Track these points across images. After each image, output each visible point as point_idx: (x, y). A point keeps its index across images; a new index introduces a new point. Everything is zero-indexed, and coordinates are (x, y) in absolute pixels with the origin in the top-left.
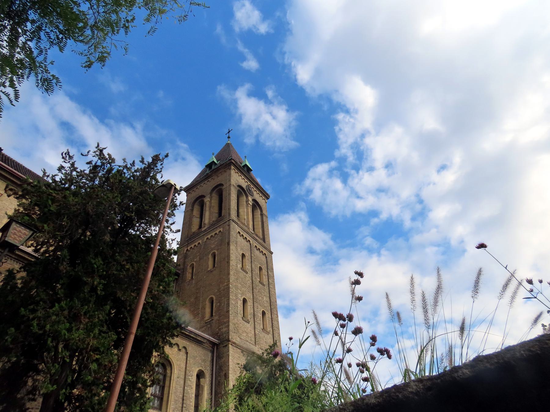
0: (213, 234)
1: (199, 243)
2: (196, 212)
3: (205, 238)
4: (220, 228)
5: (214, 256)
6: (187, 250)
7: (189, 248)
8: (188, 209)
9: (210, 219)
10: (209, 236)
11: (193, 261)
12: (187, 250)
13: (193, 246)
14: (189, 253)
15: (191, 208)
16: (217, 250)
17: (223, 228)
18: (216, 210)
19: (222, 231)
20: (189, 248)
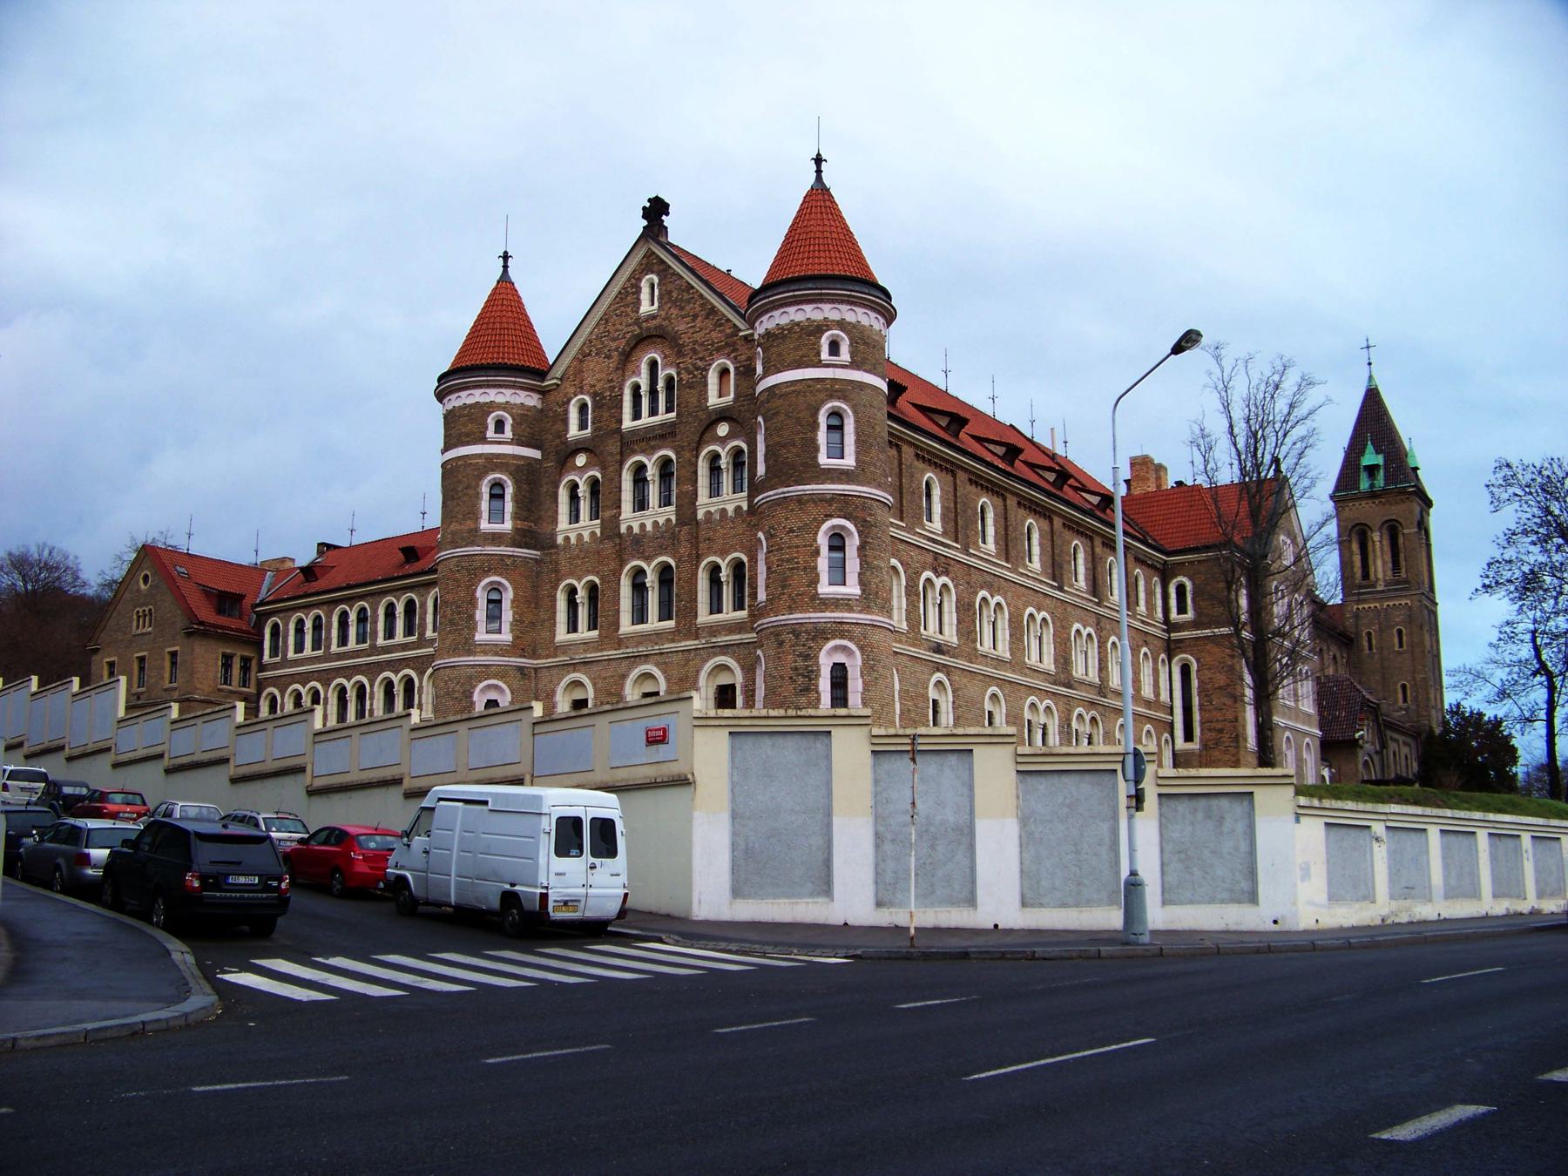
5: (1400, 632)
9: (1384, 572)
12: (1358, 609)
13: (1366, 606)
14: (1361, 614)
18: (1388, 558)
20: (1360, 607)
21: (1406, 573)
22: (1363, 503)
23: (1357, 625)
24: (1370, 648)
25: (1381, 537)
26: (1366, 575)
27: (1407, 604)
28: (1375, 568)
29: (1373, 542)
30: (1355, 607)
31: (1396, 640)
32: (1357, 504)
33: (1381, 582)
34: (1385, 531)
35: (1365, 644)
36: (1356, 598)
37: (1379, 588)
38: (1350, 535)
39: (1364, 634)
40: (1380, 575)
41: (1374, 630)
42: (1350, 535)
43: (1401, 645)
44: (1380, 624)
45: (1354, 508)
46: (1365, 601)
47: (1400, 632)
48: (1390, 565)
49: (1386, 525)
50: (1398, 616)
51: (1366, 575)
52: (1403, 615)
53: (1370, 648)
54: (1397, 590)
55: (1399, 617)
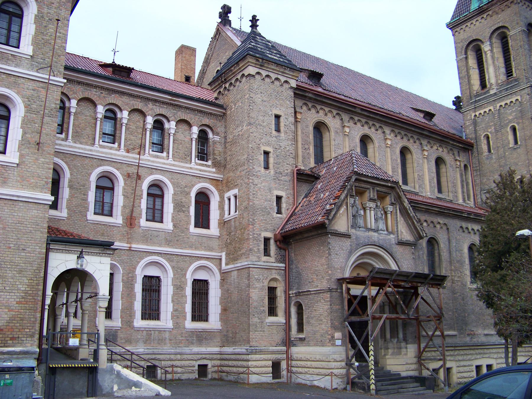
0: (508, 102)
1: (490, 110)
2: (472, 62)
3: (498, 105)
4: (517, 96)
5: (514, 129)
6: (475, 116)
7: (477, 114)
8: (461, 57)
9: (496, 77)
10: (503, 104)
11: (486, 130)
12: (475, 116)
13: (482, 112)
14: (479, 120)
15: (465, 56)
16: (518, 123)
17: (521, 96)
19: (520, 100)
20: (477, 114)
21: (515, 72)
22: (474, 21)
23: (475, 130)
24: (489, 151)
25: (491, 45)
26: (483, 85)
27: (517, 100)
28: (489, 77)
29: (485, 53)
30: (473, 115)
31: (511, 137)
32: (469, 24)
33: (494, 87)
34: (494, 40)
35: (485, 147)
36: (473, 106)
37: (492, 92)
38: (466, 53)
39: (482, 138)
40: (493, 81)
41: (490, 132)
42: (466, 53)
43: (516, 142)
44: (495, 125)
45: (467, 29)
46: (481, 107)
47: (514, 129)
48: (503, 70)
49: (496, 34)
50: (511, 114)
51: (483, 85)
52: (514, 112)
53: (489, 151)
54: (507, 89)
55: (510, 115)
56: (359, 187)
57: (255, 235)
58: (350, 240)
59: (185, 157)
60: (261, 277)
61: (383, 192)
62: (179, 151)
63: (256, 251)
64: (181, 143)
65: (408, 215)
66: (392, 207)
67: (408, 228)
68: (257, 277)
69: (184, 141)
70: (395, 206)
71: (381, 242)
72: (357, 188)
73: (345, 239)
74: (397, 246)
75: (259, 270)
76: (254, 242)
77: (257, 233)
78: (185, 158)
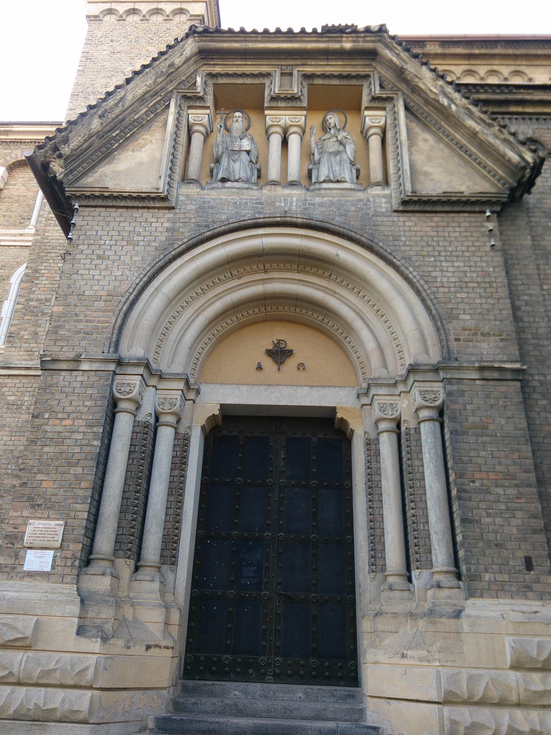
56: (227, 75)
57: (31, 303)
58: (169, 215)
59: (22, 221)
60: (26, 398)
61: (331, 76)
62: (11, 213)
63: (26, 337)
64: (17, 201)
65: (442, 111)
66: (382, 113)
67: (456, 159)
68: (13, 398)
69: (25, 196)
70: (389, 106)
71: (317, 215)
72: (221, 81)
73: (147, 214)
74: (395, 218)
75: (24, 380)
76: (26, 318)
77: (40, 297)
78: (21, 223)
